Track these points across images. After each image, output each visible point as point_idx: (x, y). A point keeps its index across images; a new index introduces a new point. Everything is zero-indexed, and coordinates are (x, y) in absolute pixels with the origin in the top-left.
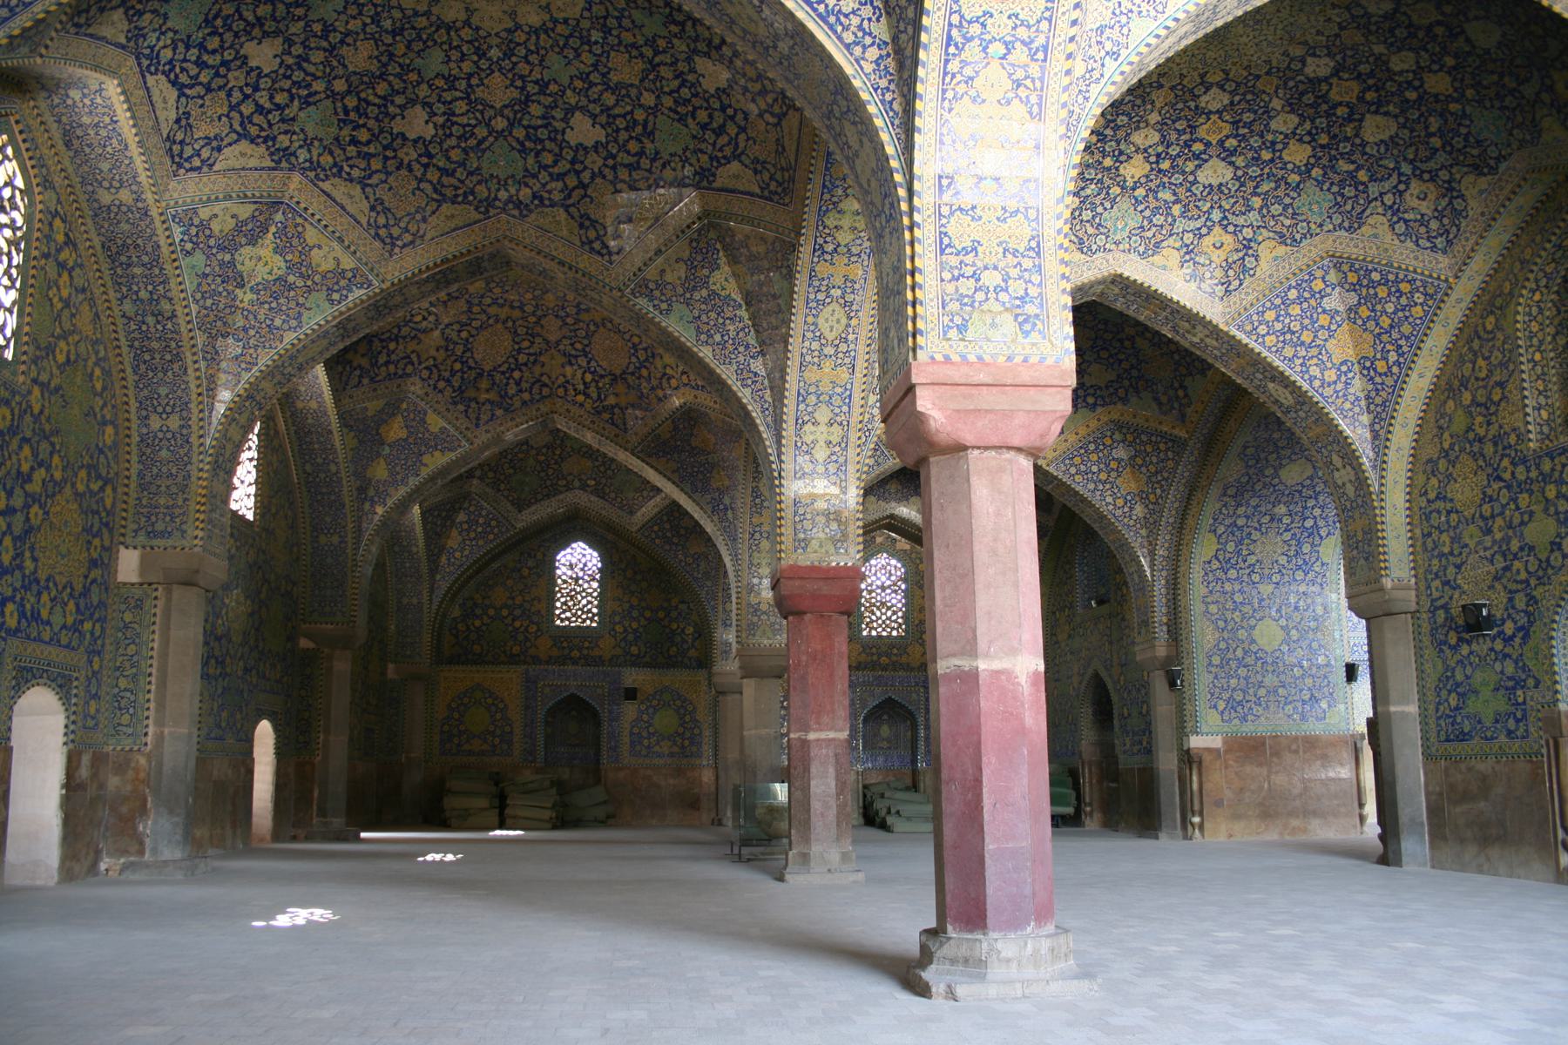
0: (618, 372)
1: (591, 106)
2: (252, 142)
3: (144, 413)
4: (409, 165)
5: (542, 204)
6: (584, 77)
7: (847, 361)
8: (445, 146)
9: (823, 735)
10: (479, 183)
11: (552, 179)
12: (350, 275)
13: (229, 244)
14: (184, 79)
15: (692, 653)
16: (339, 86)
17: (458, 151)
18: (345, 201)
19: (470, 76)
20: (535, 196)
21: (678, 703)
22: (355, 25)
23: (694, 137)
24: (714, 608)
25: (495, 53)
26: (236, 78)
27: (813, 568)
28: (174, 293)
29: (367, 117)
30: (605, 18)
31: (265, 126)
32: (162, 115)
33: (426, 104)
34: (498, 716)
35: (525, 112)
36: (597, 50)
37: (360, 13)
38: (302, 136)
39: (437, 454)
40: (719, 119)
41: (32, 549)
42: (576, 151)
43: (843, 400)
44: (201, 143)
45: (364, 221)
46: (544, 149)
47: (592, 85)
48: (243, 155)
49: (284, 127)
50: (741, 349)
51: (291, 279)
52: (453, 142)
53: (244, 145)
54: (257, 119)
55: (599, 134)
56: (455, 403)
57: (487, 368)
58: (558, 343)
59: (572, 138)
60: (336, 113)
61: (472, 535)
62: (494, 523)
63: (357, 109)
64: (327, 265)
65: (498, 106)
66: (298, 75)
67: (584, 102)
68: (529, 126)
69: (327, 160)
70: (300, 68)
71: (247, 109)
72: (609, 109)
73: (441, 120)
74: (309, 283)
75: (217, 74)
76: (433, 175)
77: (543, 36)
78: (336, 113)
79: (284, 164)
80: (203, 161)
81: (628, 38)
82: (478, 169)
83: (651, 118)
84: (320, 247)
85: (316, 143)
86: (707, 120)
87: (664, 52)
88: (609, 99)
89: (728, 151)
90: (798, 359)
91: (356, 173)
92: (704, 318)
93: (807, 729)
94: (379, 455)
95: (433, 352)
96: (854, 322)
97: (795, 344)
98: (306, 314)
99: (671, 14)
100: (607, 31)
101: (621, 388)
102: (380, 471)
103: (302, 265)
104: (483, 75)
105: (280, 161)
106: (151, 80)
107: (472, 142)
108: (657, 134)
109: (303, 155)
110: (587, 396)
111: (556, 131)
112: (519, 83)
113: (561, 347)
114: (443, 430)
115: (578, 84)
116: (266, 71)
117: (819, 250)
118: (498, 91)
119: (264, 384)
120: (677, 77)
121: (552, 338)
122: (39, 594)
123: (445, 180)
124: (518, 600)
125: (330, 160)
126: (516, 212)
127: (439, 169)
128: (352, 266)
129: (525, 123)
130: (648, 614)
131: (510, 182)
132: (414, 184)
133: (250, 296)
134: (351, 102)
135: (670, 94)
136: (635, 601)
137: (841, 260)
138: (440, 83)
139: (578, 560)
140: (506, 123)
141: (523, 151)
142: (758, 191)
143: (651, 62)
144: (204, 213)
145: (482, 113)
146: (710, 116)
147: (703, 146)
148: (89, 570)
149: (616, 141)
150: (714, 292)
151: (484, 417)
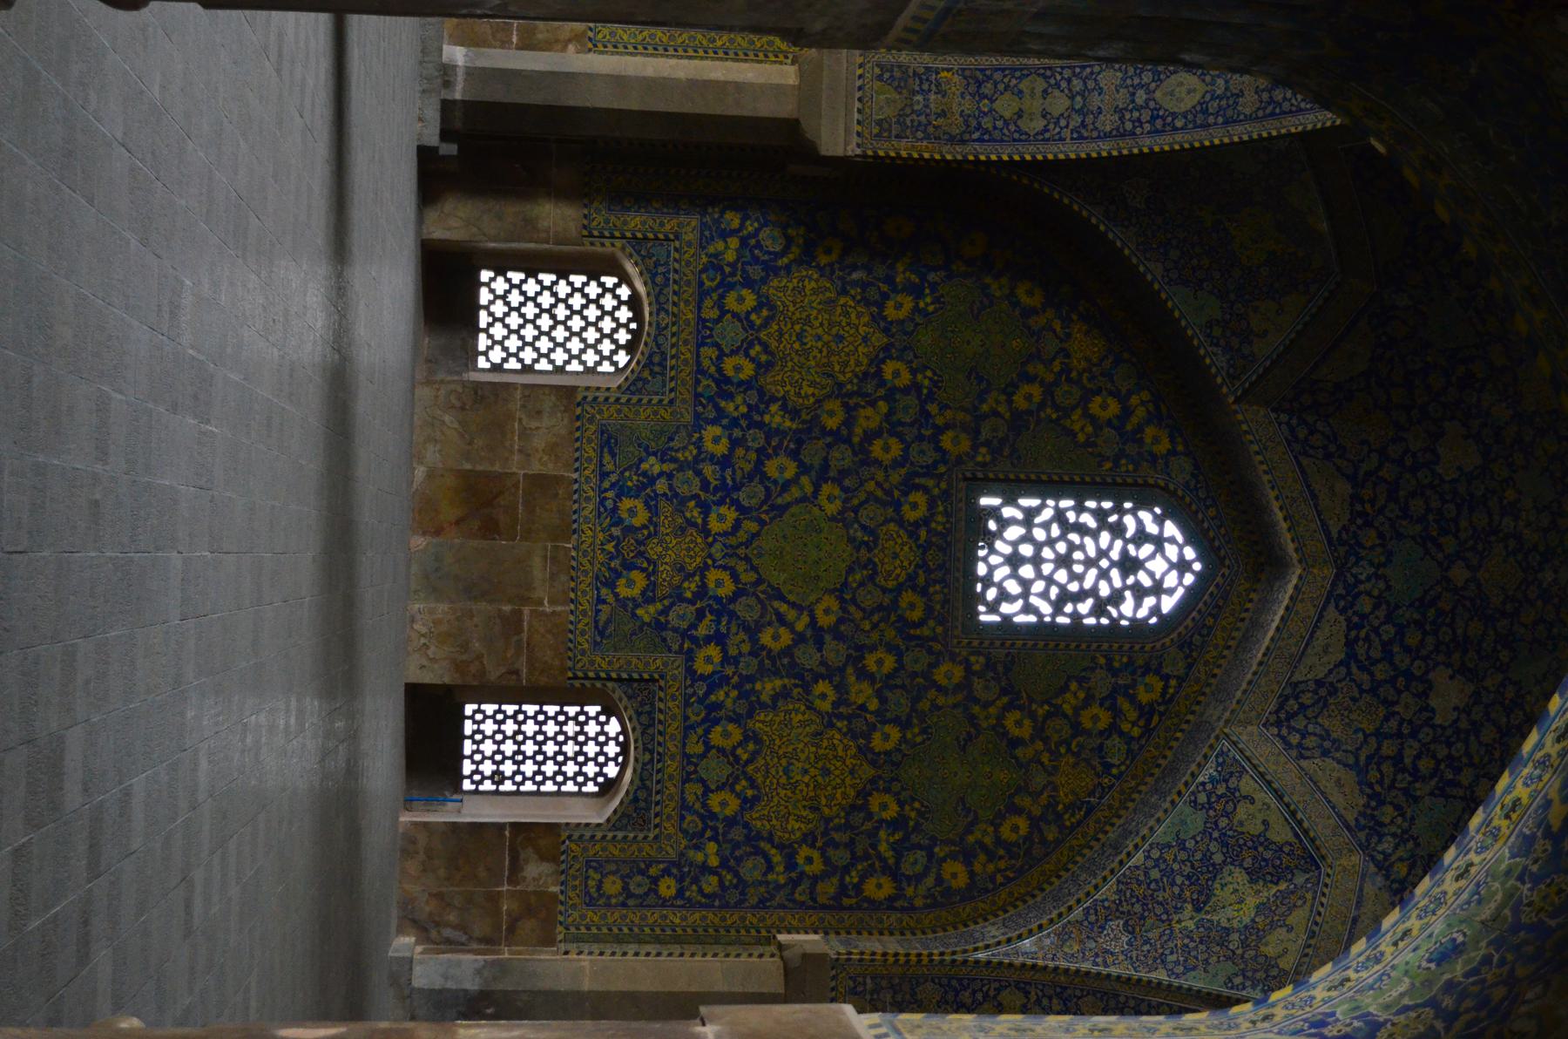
14: (1361, 649)
26: (1407, 707)
31: (1387, 782)
41: (784, 694)
44: (1318, 730)
49: (1401, 800)
53: (1350, 778)
54: (1387, 768)
64: (1270, 950)
79: (1362, 835)
80: (1300, 745)
84: (1290, 929)
85: (1410, 845)
98: (1199, 973)
105: (1362, 828)
106: (1331, 607)
109: (1387, 845)
116: (1438, 721)
122: (736, 719)
125: (1404, 871)
133: (1191, 925)
144: (1247, 785)
148: (780, 847)
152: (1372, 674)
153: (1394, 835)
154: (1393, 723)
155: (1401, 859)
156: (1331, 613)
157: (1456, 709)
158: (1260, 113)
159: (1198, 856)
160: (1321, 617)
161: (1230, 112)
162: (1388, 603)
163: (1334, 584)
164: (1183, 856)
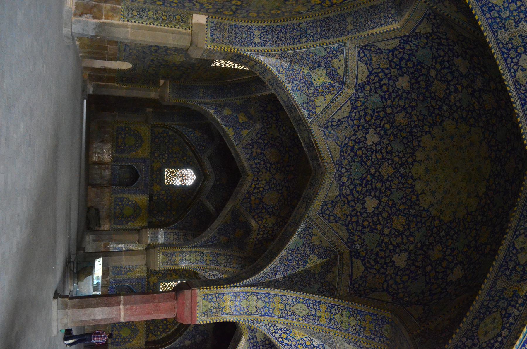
0: (264, 200)
1: (382, 207)
2: (368, 76)
3: (261, 29)
4: (356, 135)
5: (341, 186)
6: (394, 205)
7: (284, 315)
8: (363, 149)
9: (122, 312)
10: (349, 161)
11: (350, 190)
12: (313, 111)
13: (327, 65)
14: (396, 52)
15: (154, 220)
16: (389, 110)
17: (361, 154)
18: (342, 110)
19: (392, 160)
20: (344, 183)
22: (415, 118)
23: (372, 250)
24: (171, 229)
25: (402, 170)
26: (394, 72)
27: (196, 303)
28: (309, 44)
29: (375, 120)
30: (421, 216)
31: (374, 81)
32: (383, 43)
33: (380, 142)
34: (132, 148)
35: (378, 181)
36: (406, 211)
37: (419, 120)
38: (369, 95)
39: (233, 133)
40: (382, 261)
42: (362, 200)
43: (267, 312)
44: (369, 57)
45: (334, 117)
46: (363, 187)
47: (391, 208)
48: (363, 73)
49: (373, 88)
50: (286, 268)
51: (312, 88)
52: (365, 152)
53: (367, 73)
54: (377, 79)
55: (370, 210)
56: (252, 140)
57: (265, 152)
58: (274, 179)
59: (368, 199)
60: (377, 108)
62: (204, 148)
63: (379, 116)
64: (317, 102)
65: (380, 170)
66: (394, 95)
67: (383, 205)
68: (372, 182)
69: (359, 104)
70: (397, 96)
71: (381, 75)
72: (381, 214)
73: (374, 148)
74: (311, 95)
75: (396, 65)
76: (351, 144)
77: (410, 190)
78: (377, 108)
79: (358, 88)
80: (362, 57)
81: (413, 225)
82: (354, 161)
83: (379, 232)
84: (325, 100)
85: (366, 100)
86: (380, 256)
87: (408, 240)
88: (385, 215)
89: (368, 265)
90: (284, 294)
91: (353, 115)
92: (298, 252)
93: (124, 305)
95: (271, 133)
96: (300, 319)
97: (290, 294)
99: (426, 245)
100: (415, 216)
101: (257, 201)
102: (227, 112)
103: (317, 93)
104: (393, 165)
105: (359, 86)
106: (399, 39)
107: (365, 159)
108: (372, 234)
109: (361, 95)
110: (254, 188)
111: (370, 192)
112: (390, 179)
113: (273, 180)
114: (242, 136)
115: (391, 203)
116: (396, 83)
117: (332, 306)
118: (386, 171)
119: (270, 76)
120: (397, 244)
121: (276, 176)
123: (349, 148)
124: (175, 156)
125: (359, 105)
126: (337, 175)
127: (354, 146)
128: (317, 112)
129: (373, 180)
130: (169, 203)
131: (349, 173)
132: (348, 136)
133: (306, 72)
134: (382, 114)
135: (390, 240)
137: (327, 315)
138: (389, 148)
139: (188, 177)
140: (373, 173)
141: (362, 179)
142: (354, 278)
143: (403, 233)
144: (341, 57)
145: (377, 164)
146: (382, 258)
147: (369, 253)
149: (368, 216)
150: (309, 256)
151: (246, 151)
152: (393, 58)
153: (365, 94)
154: (388, 71)
155: (361, 101)
156: (397, 40)
157: (402, 87)
158: (501, 45)
159: (318, 60)
160: (394, 39)
161: (495, 26)
162: (413, 53)
163: (405, 36)
164: (314, 57)
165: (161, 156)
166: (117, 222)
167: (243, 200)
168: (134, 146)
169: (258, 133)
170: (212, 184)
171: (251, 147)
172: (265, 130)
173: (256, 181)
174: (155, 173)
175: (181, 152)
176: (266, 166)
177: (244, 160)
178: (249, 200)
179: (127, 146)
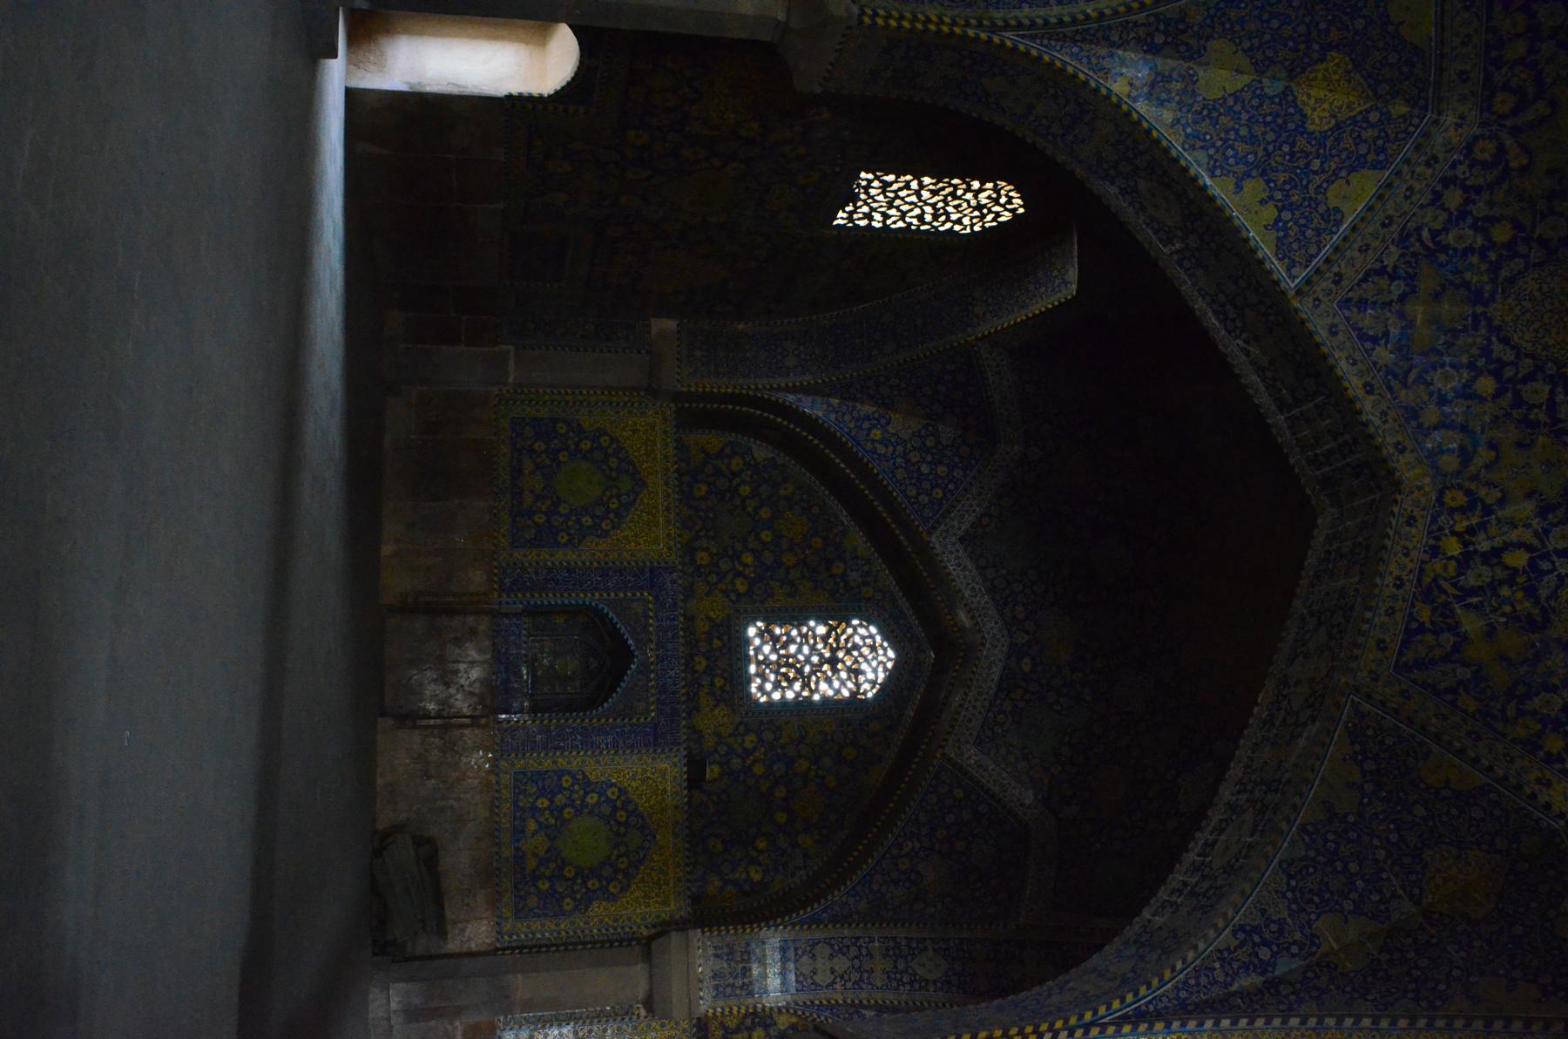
15: (715, 883)
21: (623, 863)
24: (815, 921)
39: (1270, 213)
61: (914, 456)
62: (938, 493)
94: (1260, 68)
110: (1464, 561)
114: (1333, 217)
124: (788, 559)
130: (780, 792)
136: (803, 765)
151: (1367, 319)
165: (724, 565)
166: (533, 902)
167: (1405, 644)
168: (599, 511)
169: (1446, 182)
170: (997, 671)
171: (1398, 288)
172: (1501, 149)
173: (1462, 510)
174: (703, 646)
175: (817, 542)
176: (1518, 402)
177: (1354, 384)
178: (1448, 639)
179: (564, 509)
